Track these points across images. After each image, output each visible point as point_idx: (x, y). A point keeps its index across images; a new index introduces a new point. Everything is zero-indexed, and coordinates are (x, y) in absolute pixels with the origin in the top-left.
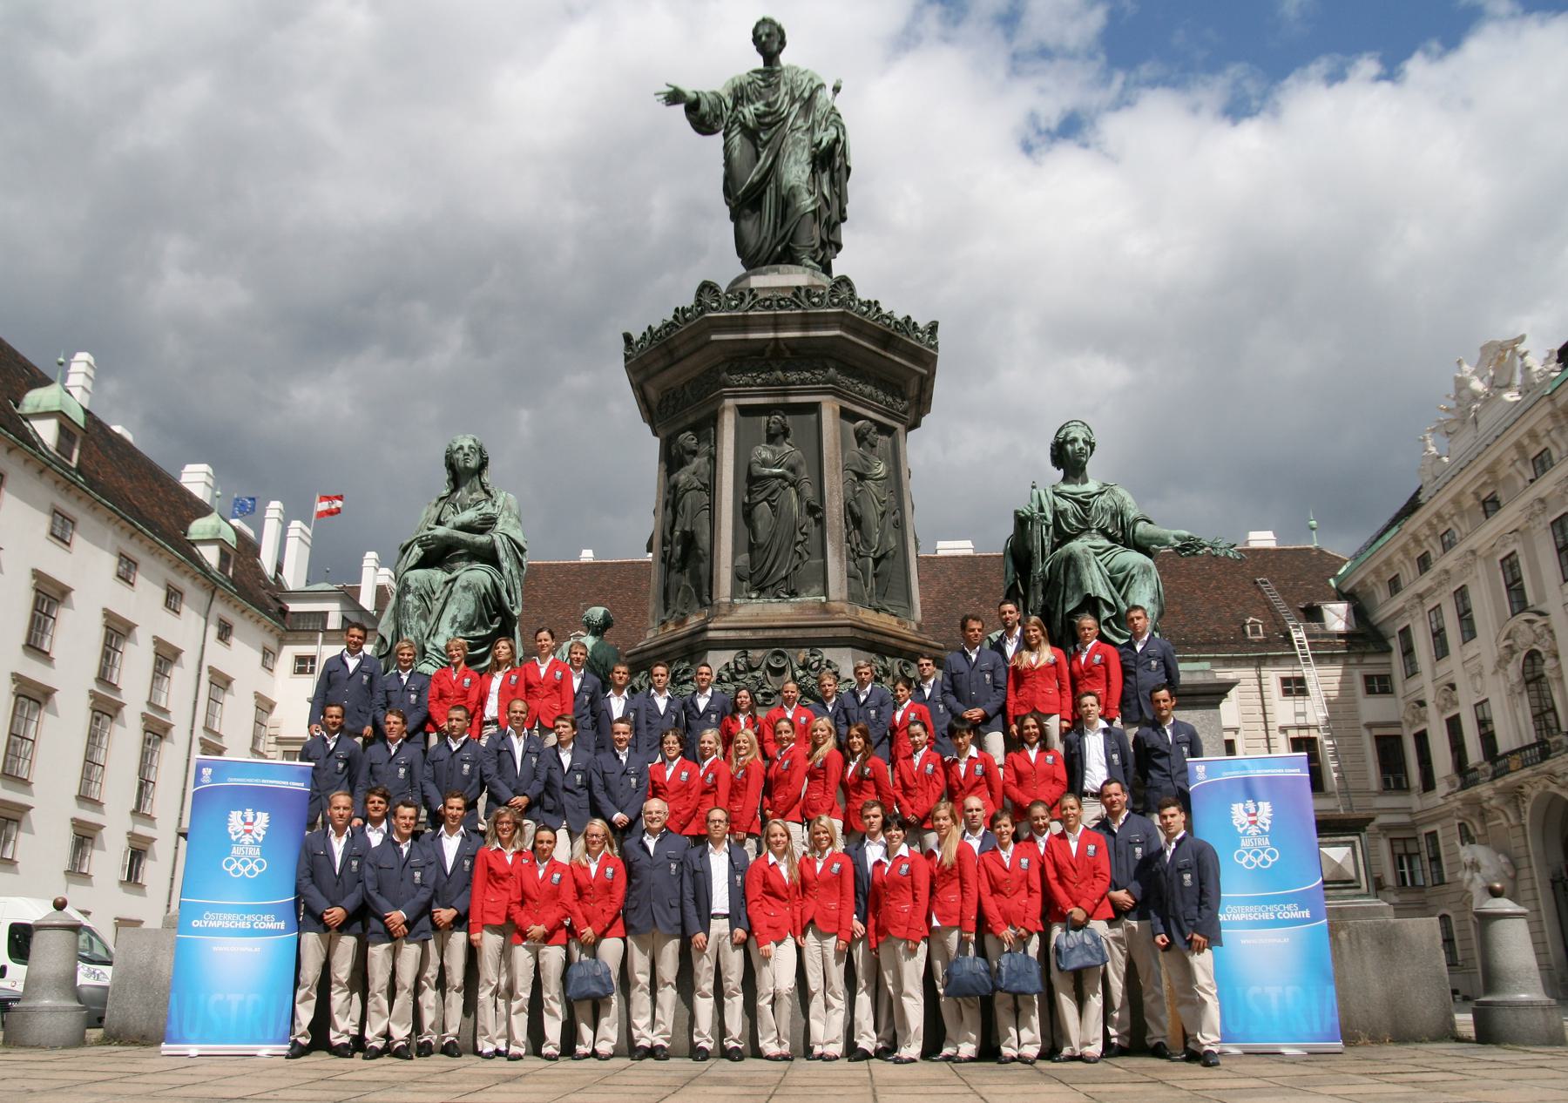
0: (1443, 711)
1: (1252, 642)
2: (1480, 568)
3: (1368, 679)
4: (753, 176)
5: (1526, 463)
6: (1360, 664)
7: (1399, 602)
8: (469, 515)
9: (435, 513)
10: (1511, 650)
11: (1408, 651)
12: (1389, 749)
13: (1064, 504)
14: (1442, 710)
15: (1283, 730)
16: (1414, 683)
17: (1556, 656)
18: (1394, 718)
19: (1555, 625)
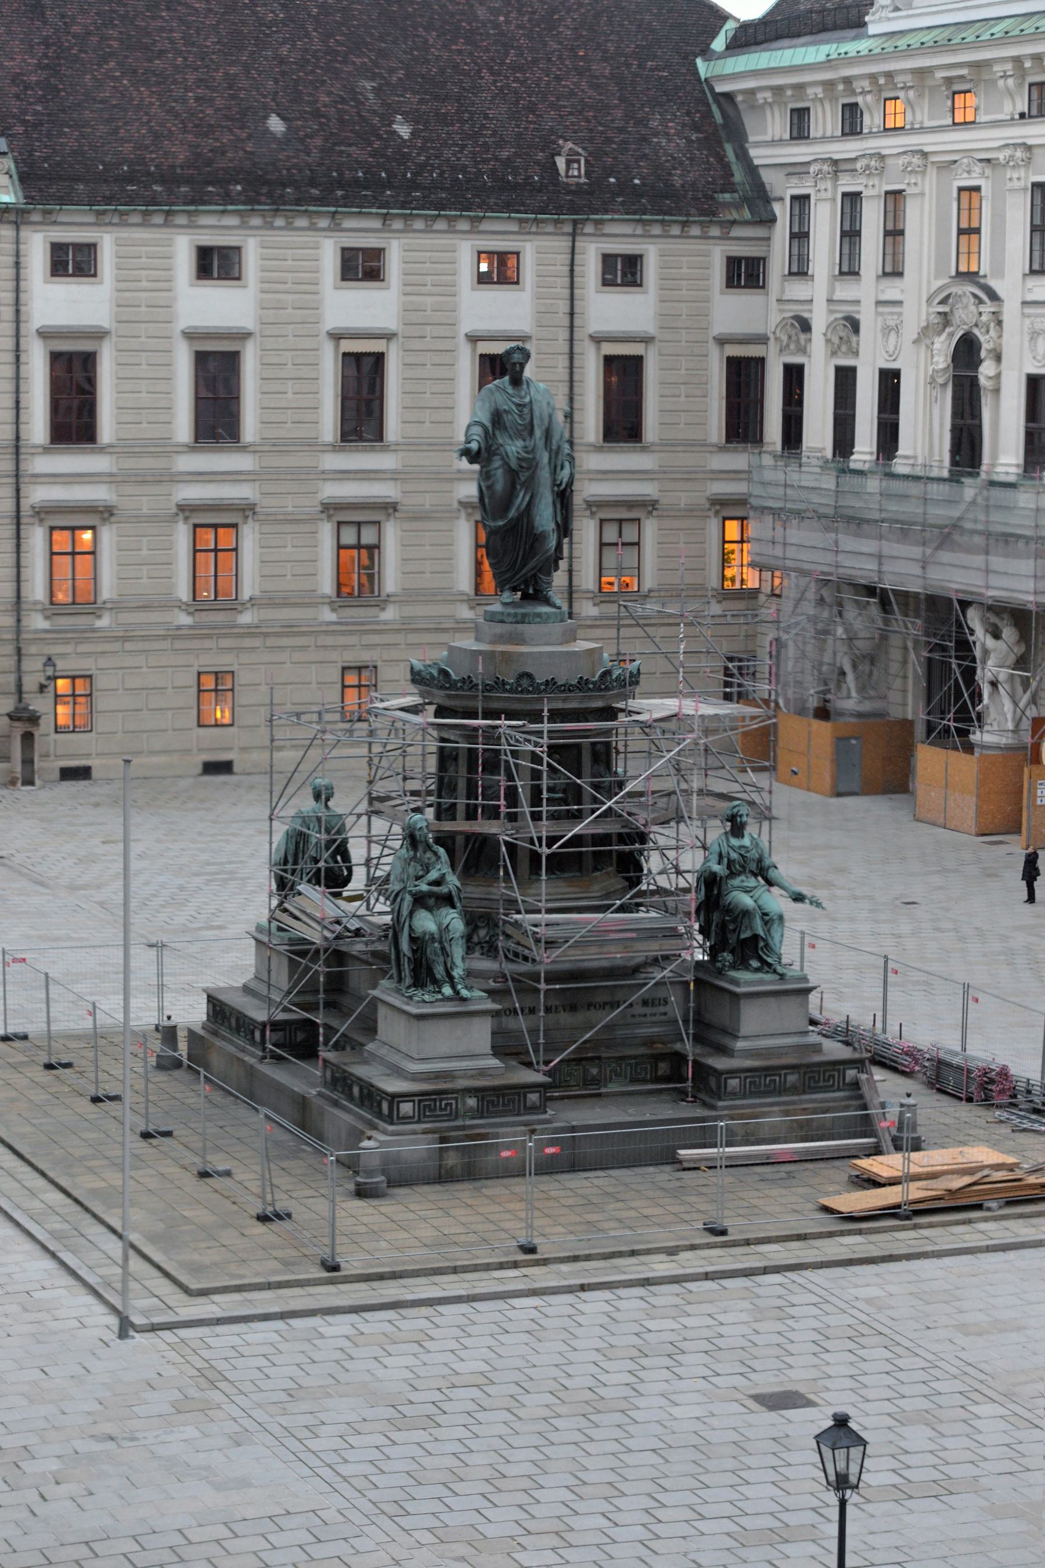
0: (834, 354)
1: (568, 189)
2: (930, 182)
3: (733, 264)
4: (512, 513)
5: (1020, 85)
6: (725, 237)
7: (800, 152)
8: (433, 875)
9: (411, 870)
10: (946, 319)
11: (800, 236)
12: (743, 377)
13: (734, 855)
14: (834, 354)
15: (598, 340)
16: (798, 290)
17: (998, 358)
18: (757, 329)
19: (1006, 318)
